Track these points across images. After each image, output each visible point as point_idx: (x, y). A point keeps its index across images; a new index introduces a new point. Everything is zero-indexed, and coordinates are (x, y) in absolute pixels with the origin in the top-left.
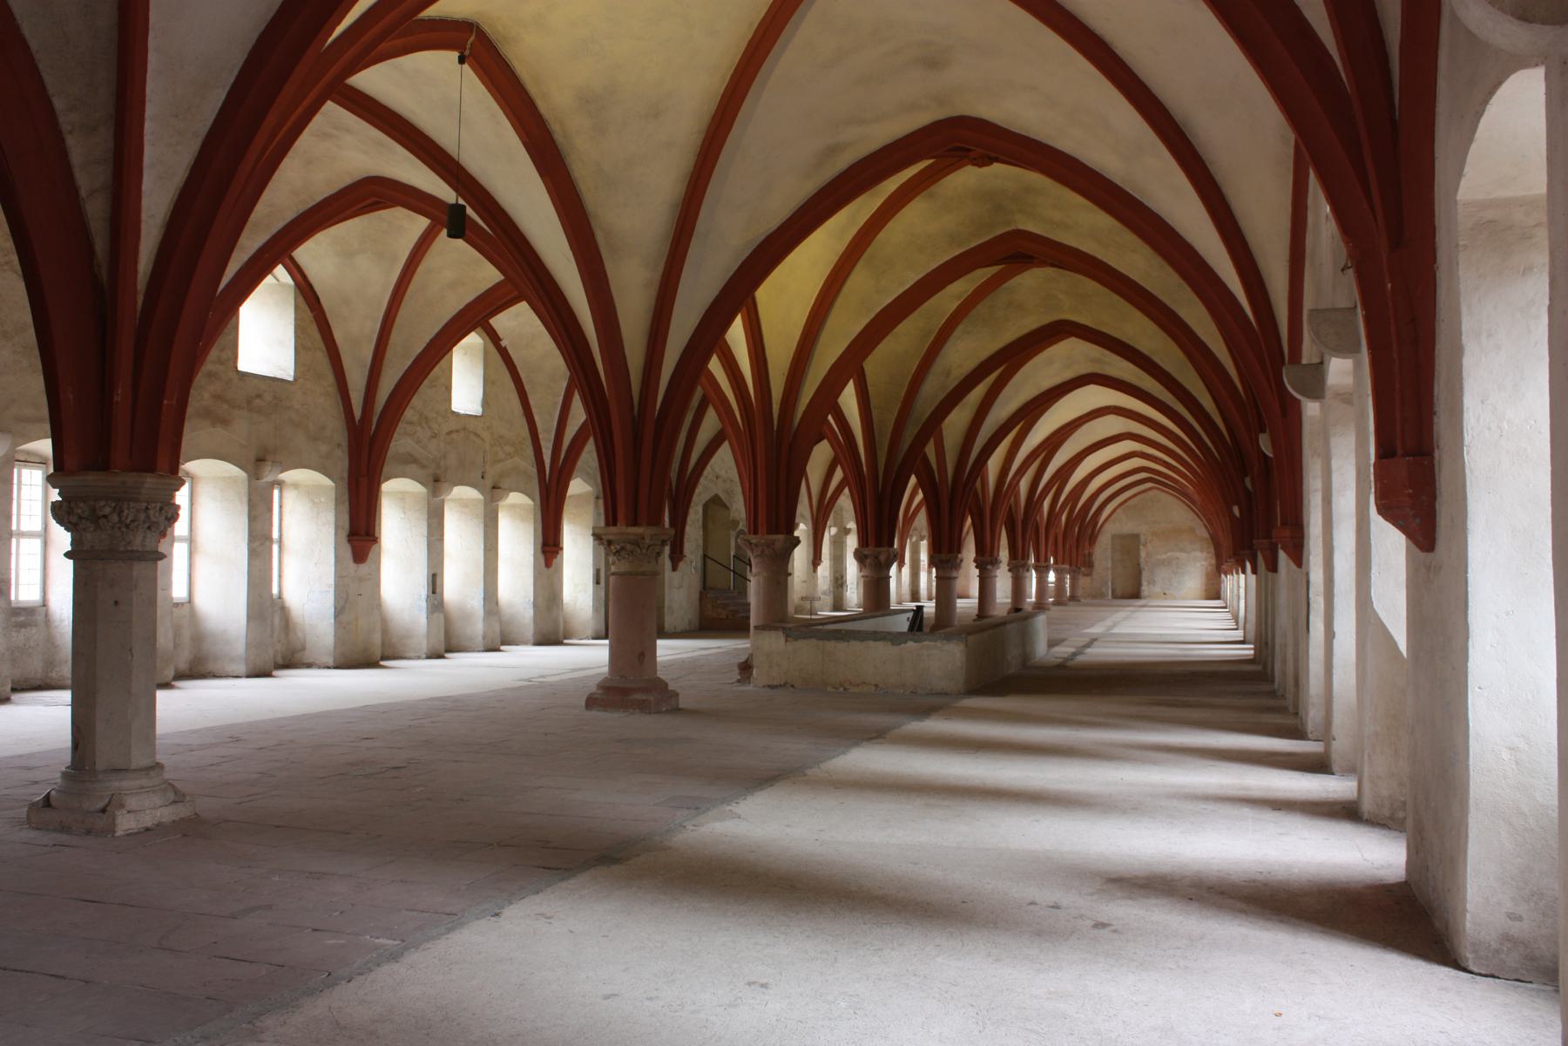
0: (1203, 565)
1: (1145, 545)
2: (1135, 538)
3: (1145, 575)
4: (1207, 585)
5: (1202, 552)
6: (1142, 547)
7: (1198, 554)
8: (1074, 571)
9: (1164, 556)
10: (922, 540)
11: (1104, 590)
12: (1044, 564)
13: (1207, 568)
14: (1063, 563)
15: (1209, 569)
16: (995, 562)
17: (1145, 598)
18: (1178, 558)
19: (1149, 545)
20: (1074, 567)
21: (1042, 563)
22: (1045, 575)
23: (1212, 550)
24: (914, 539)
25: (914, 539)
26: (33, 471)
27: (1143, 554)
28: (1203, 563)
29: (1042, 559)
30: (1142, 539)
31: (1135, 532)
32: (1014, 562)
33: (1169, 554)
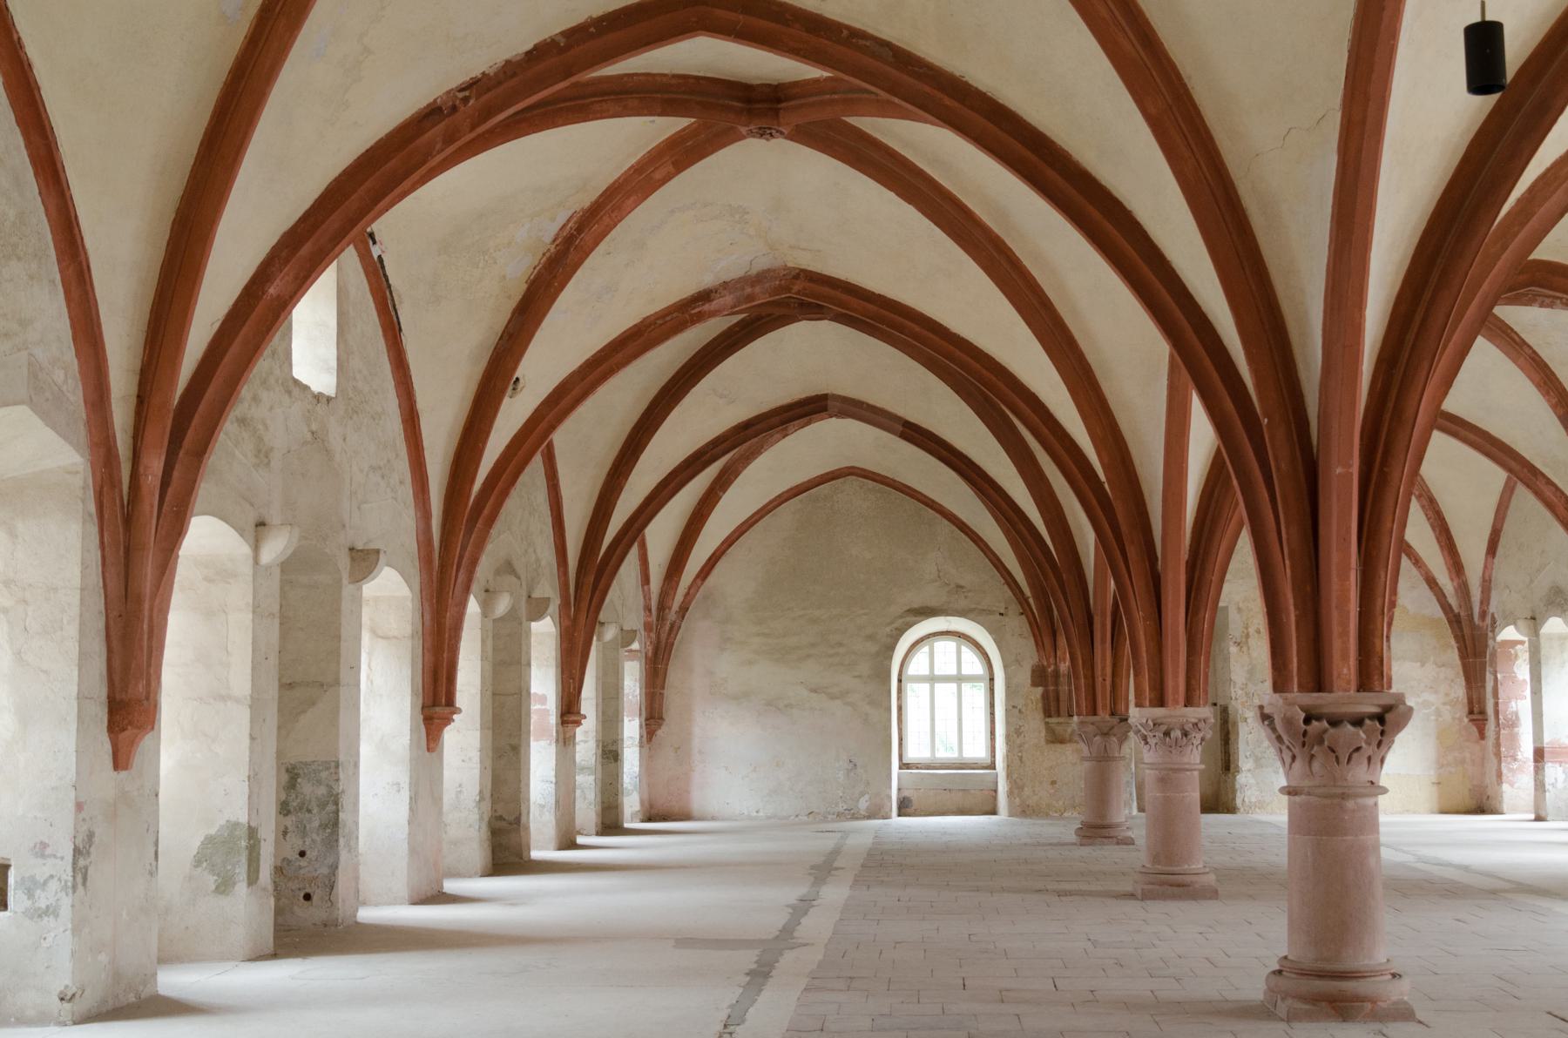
4: (1441, 763)
6: (1233, 649)
8: (1106, 734)
10: (537, 615)
12: (1368, 704)
13: (1438, 713)
14: (1189, 702)
19: (1252, 642)
20: (1104, 715)
21: (1344, 697)
22: (1358, 773)
23: (1453, 655)
24: (503, 605)
25: (503, 605)
28: (1431, 698)
29: (1344, 668)
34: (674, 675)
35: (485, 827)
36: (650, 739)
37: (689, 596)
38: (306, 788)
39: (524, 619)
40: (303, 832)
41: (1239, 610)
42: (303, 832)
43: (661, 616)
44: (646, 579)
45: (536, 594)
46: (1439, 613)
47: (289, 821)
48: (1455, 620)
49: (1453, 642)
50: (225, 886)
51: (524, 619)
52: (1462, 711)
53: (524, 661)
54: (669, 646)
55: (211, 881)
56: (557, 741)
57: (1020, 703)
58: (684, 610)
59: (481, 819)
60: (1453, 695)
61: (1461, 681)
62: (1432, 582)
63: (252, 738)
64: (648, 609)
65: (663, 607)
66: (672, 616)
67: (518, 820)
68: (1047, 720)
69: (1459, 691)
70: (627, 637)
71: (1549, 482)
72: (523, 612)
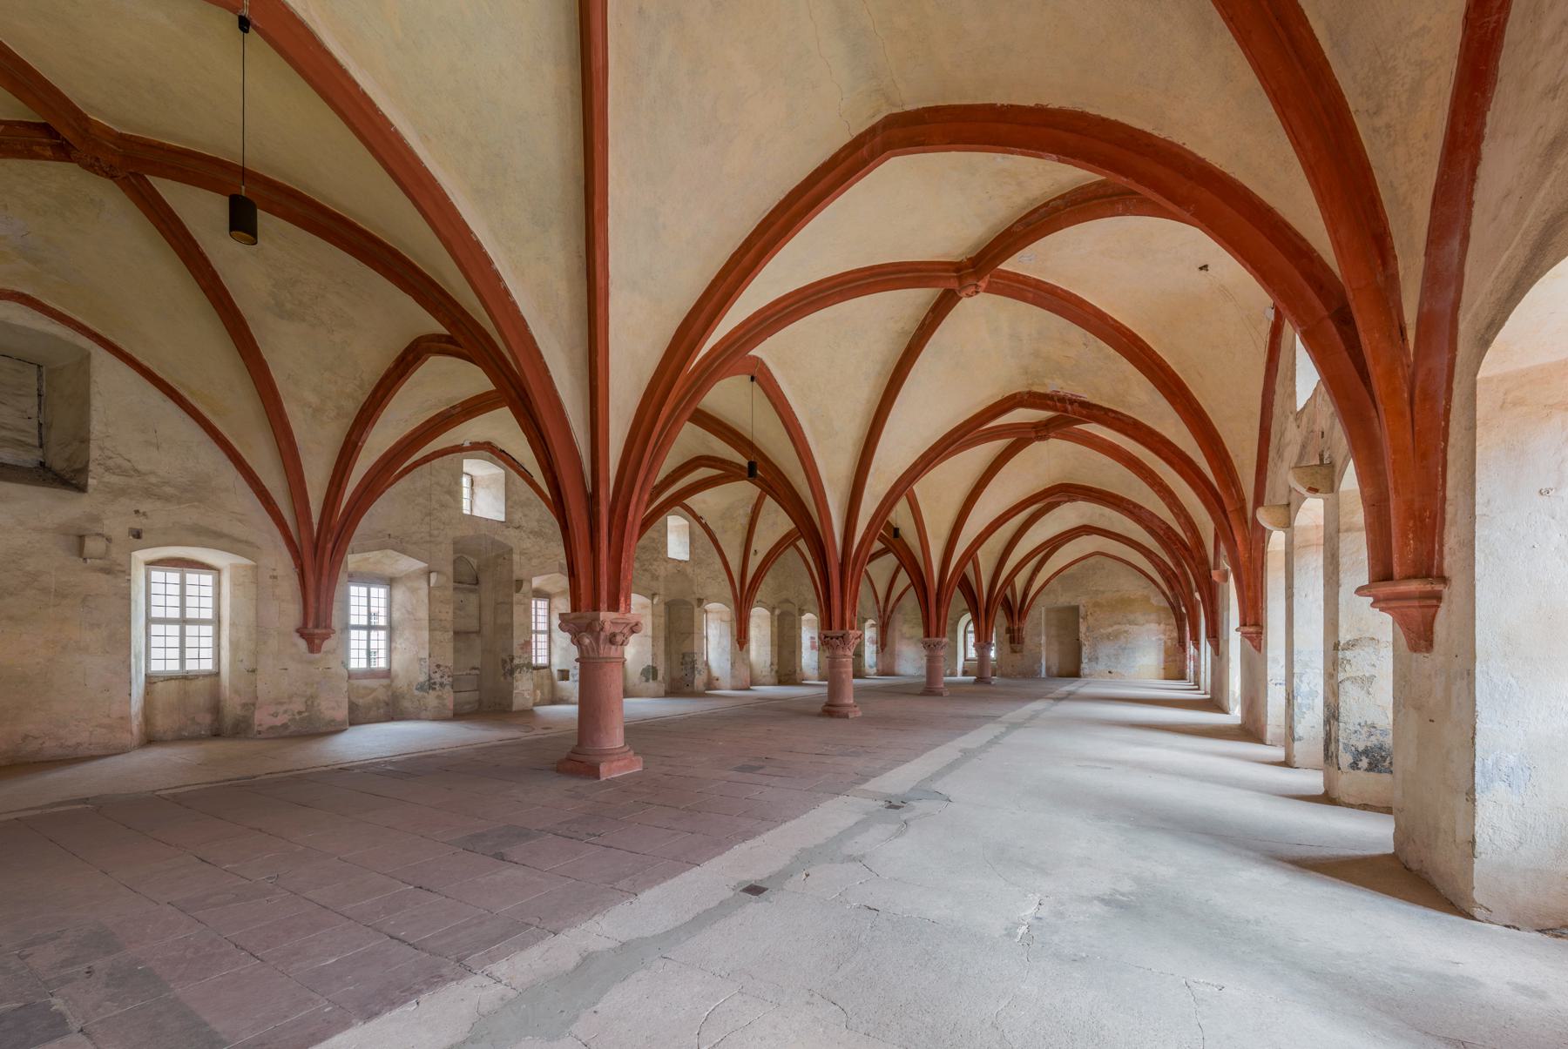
0: (1160, 639)
1: (1085, 618)
2: (1075, 610)
3: (1085, 651)
4: (1165, 662)
5: (1159, 624)
6: (1081, 620)
7: (1154, 626)
9: (1110, 630)
11: (1036, 667)
13: (1165, 642)
15: (1169, 643)
16: (989, 644)
17: (1085, 676)
18: (1126, 632)
24: (777, 612)
26: (361, 588)
27: (1083, 628)
28: (1162, 637)
30: (1082, 611)
31: (1073, 603)
32: (927, 639)
33: (1116, 627)
34: (890, 632)
35: (773, 673)
36: (882, 650)
37: (894, 607)
38: (687, 659)
39: (797, 615)
40: (686, 669)
41: (1084, 606)
42: (686, 669)
43: (885, 610)
44: (878, 602)
45: (805, 608)
46: (1167, 605)
47: (683, 667)
48: (1173, 607)
49: (1173, 616)
50: (647, 680)
51: (797, 615)
52: (1176, 642)
53: (797, 627)
54: (888, 623)
55: (644, 679)
56: (819, 650)
57: (1001, 639)
58: (892, 612)
59: (772, 670)
60: (1172, 636)
61: (1176, 630)
62: (1164, 593)
63: (653, 646)
64: (879, 611)
65: (885, 610)
66: (888, 613)
67: (795, 672)
68: (1013, 645)
69: (1175, 634)
70: (865, 620)
71: (1157, 556)
72: (797, 613)
